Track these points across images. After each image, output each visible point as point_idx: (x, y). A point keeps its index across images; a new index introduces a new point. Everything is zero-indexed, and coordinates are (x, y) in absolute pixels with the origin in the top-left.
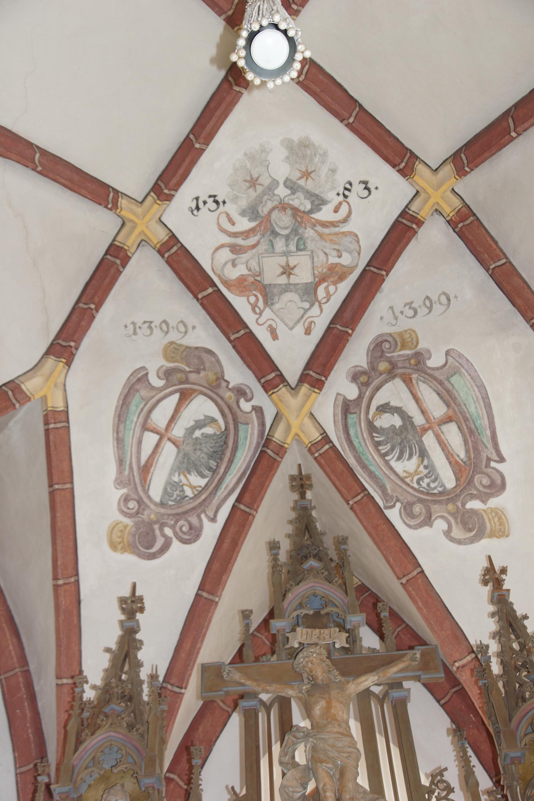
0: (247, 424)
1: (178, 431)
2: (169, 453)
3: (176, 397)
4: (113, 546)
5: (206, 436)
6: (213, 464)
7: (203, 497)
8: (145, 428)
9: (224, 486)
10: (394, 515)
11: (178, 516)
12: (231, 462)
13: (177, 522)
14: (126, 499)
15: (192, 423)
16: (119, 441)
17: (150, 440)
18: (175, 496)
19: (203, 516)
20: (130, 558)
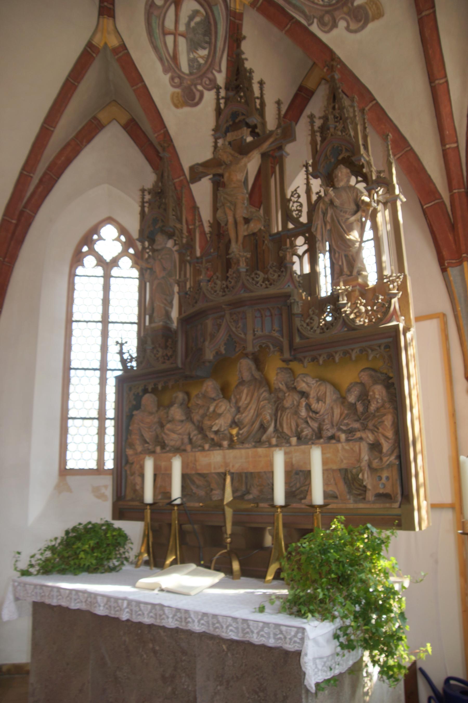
0: (216, 5)
1: (182, 28)
2: (182, 42)
3: (172, 8)
4: (176, 106)
5: (197, 24)
6: (207, 39)
7: (210, 60)
8: (165, 33)
9: (218, 49)
10: (315, 28)
11: (201, 77)
12: (216, 33)
13: (202, 80)
14: (172, 79)
15: (187, 19)
16: (155, 48)
17: (170, 39)
18: (195, 66)
19: (214, 72)
20: (187, 109)
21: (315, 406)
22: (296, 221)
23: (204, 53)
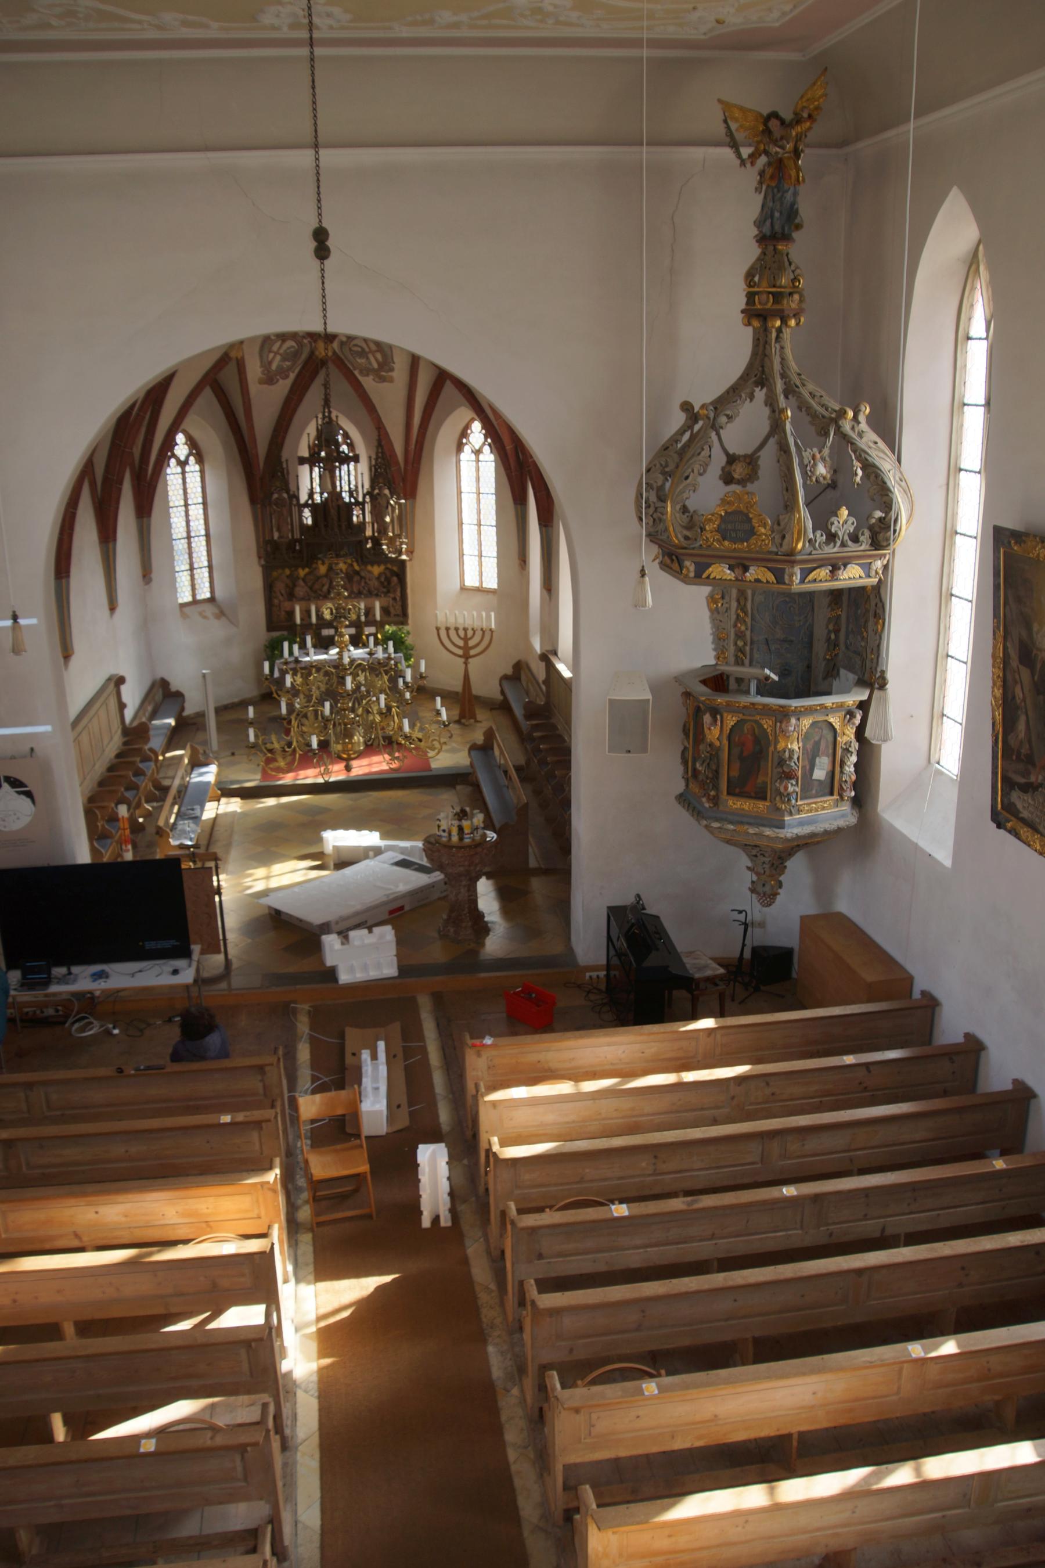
1: (281, 351)
2: (278, 358)
4: (260, 383)
8: (270, 351)
10: (356, 373)
20: (266, 386)
23: (288, 363)
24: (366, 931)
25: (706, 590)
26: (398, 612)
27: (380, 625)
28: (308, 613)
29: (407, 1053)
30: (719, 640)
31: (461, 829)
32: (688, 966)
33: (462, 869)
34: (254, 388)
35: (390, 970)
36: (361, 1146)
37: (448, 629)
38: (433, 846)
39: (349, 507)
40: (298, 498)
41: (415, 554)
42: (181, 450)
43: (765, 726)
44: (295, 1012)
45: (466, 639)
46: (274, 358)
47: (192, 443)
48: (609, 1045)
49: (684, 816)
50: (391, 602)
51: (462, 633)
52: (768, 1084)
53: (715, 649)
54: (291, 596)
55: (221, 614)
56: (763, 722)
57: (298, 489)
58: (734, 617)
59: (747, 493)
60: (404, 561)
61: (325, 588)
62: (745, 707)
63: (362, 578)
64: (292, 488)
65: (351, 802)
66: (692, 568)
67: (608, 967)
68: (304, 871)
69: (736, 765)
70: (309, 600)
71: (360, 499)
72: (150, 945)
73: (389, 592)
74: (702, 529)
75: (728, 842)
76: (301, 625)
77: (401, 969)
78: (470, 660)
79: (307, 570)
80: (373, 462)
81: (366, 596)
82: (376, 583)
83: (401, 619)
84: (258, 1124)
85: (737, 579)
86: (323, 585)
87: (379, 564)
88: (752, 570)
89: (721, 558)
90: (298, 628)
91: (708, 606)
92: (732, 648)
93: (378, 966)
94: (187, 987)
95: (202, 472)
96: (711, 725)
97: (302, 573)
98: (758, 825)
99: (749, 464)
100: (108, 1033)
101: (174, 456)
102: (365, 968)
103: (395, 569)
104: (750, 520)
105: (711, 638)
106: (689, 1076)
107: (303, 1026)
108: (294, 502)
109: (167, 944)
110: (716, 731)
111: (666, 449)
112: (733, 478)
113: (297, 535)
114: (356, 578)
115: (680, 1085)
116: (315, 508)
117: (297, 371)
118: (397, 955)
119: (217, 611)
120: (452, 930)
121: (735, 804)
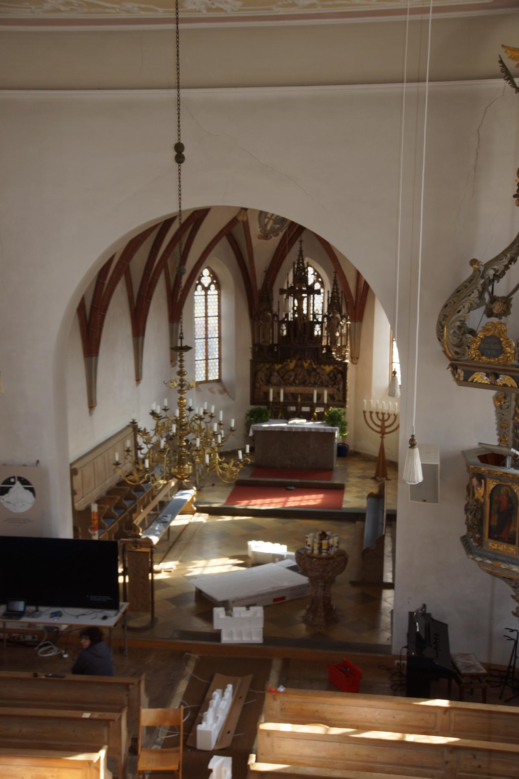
2: (271, 222)
4: (259, 238)
16: (260, 220)
17: (267, 220)
21: (322, 377)
22: (317, 320)
24: (244, 608)
25: (493, 393)
26: (340, 399)
27: (327, 406)
28: (279, 394)
29: (249, 696)
30: (502, 427)
31: (321, 545)
32: (459, 665)
33: (318, 573)
34: (255, 242)
35: (257, 638)
36: (178, 751)
37: (371, 413)
38: (301, 556)
39: (312, 325)
40: (278, 317)
41: (359, 360)
42: (206, 280)
43: (515, 491)
44: (188, 658)
45: (383, 421)
46: (268, 222)
47: (214, 276)
48: (369, 706)
49: (461, 550)
50: (336, 391)
51: (381, 416)
52: (475, 757)
53: (498, 435)
54: (268, 382)
55: (224, 391)
56: (514, 487)
57: (279, 310)
58: (513, 412)
59: (501, 324)
60: (346, 363)
61: (292, 379)
62: (501, 475)
63: (318, 373)
64: (275, 309)
65: (280, 525)
66: (462, 374)
67: (409, 658)
68: (230, 566)
69: (495, 517)
70: (280, 386)
71: (320, 320)
72: (93, 598)
73: (335, 384)
74: (469, 347)
75: (490, 573)
76: (273, 402)
77: (266, 638)
78: (385, 435)
79: (280, 366)
80: (330, 295)
81: (319, 386)
82: (327, 378)
83: (342, 403)
84: (107, 722)
85: (491, 384)
86: (291, 376)
87: (329, 364)
88: (501, 377)
89: (480, 368)
90: (271, 404)
91: (494, 403)
92: (511, 434)
93: (250, 634)
94: (110, 628)
95: (219, 295)
96: (477, 486)
97: (278, 367)
98: (509, 563)
99: (505, 303)
100: (60, 656)
101: (200, 283)
102: (240, 634)
103: (340, 368)
104: (500, 342)
105: (495, 426)
106: (410, 738)
107: (189, 670)
108: (276, 319)
109: (106, 599)
110: (481, 491)
111: (458, 292)
112: (493, 313)
113: (276, 342)
114: (313, 373)
115: (402, 743)
116: (288, 324)
117: (284, 231)
118: (264, 629)
119: (221, 389)
120: (311, 617)
121: (493, 545)
